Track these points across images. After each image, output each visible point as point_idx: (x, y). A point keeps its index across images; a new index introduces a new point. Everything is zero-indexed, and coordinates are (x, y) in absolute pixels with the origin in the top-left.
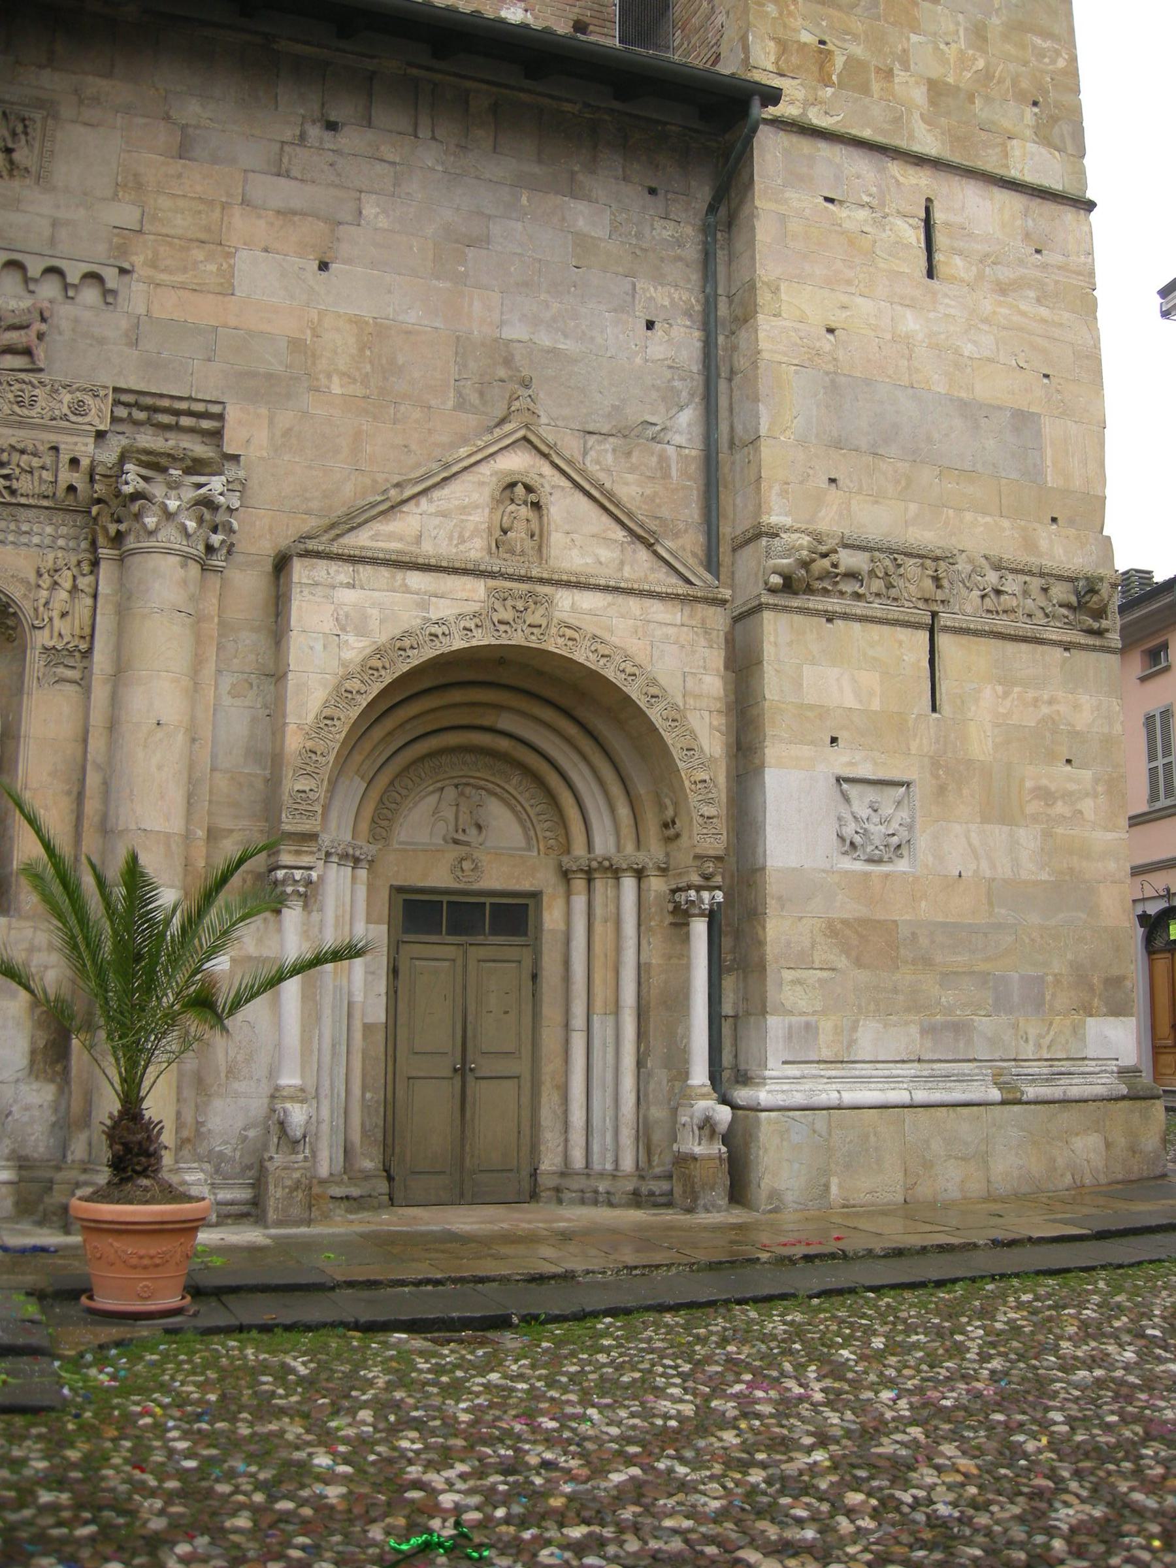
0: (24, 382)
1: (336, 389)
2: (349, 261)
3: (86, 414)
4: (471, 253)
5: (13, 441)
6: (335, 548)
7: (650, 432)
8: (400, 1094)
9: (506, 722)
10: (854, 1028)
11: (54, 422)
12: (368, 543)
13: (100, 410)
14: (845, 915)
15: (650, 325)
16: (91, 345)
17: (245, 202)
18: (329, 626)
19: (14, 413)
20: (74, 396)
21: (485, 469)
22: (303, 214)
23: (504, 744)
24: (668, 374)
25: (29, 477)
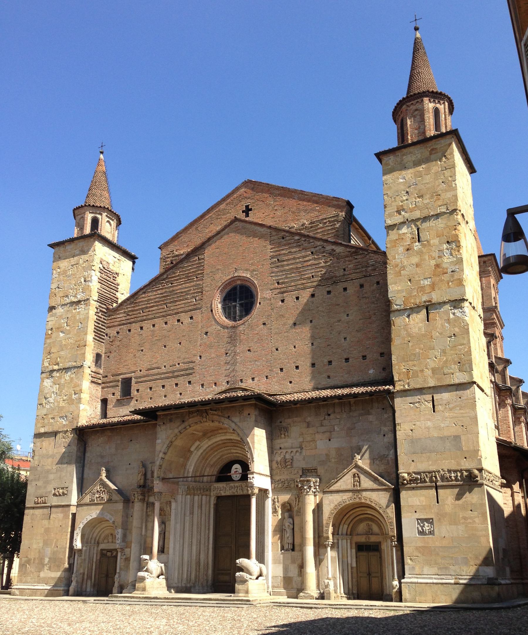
1: (333, 461)
2: (333, 438)
4: (352, 431)
6: (328, 490)
7: (385, 456)
8: (359, 580)
9: (369, 512)
10: (423, 567)
12: (333, 488)
14: (420, 545)
15: (384, 435)
17: (317, 432)
18: (328, 503)
21: (350, 472)
22: (325, 432)
23: (370, 516)
24: (388, 444)
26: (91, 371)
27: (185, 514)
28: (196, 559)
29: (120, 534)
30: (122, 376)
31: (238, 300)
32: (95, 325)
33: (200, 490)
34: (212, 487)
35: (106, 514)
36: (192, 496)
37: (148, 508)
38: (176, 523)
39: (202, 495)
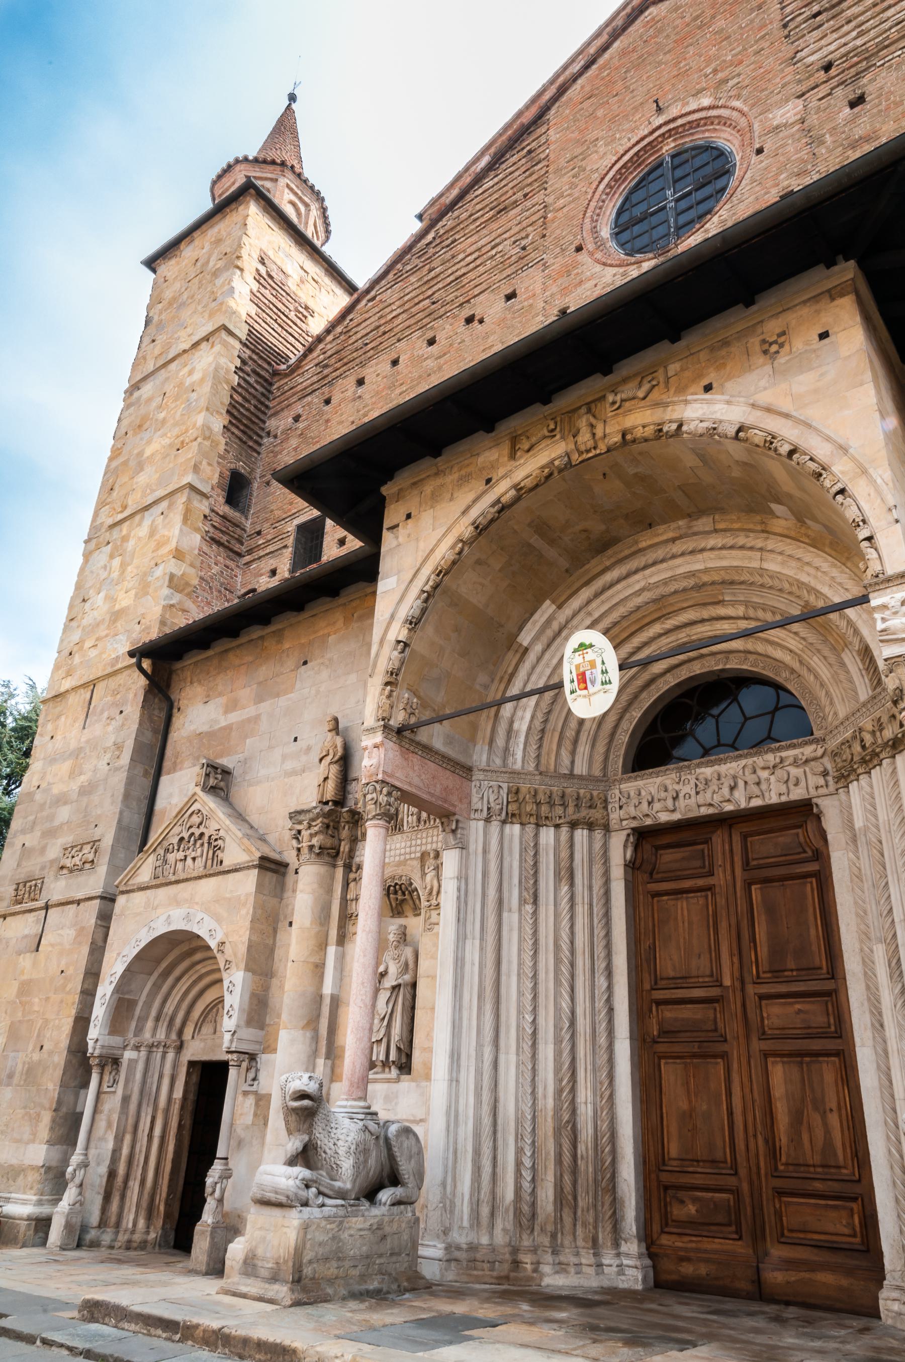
26: (213, 511)
27: (500, 902)
28: (557, 1110)
29: (238, 990)
30: (297, 522)
31: (669, 193)
32: (231, 397)
33: (564, 805)
34: (614, 794)
35: (200, 915)
36: (530, 829)
37: (352, 885)
38: (461, 938)
39: (573, 825)
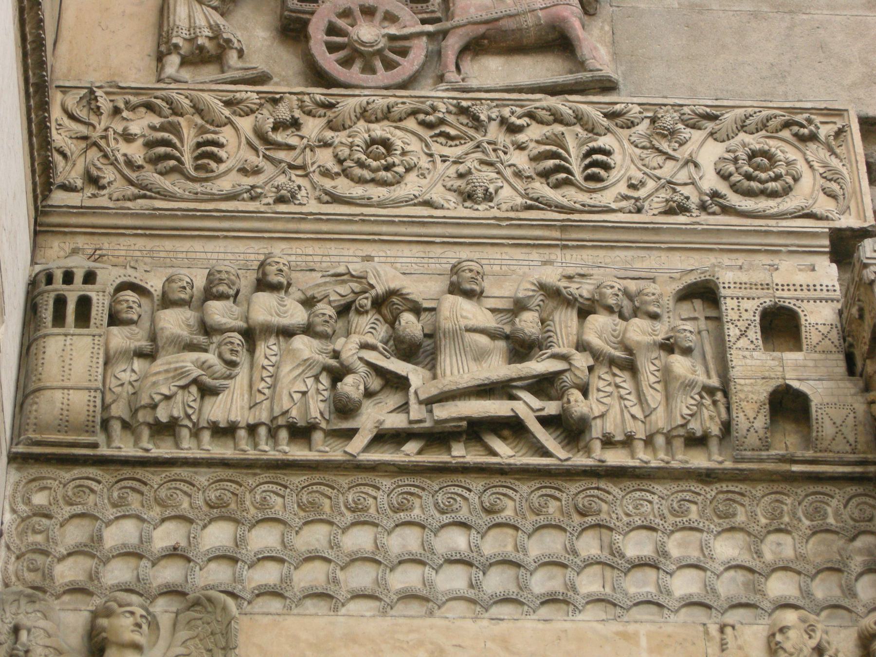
0: (558, 119)
3: (787, 190)
5: (551, 276)
11: (681, 219)
13: (832, 176)
16: (755, 15)
19: (537, 204)
20: (733, 143)
25: (624, 379)
